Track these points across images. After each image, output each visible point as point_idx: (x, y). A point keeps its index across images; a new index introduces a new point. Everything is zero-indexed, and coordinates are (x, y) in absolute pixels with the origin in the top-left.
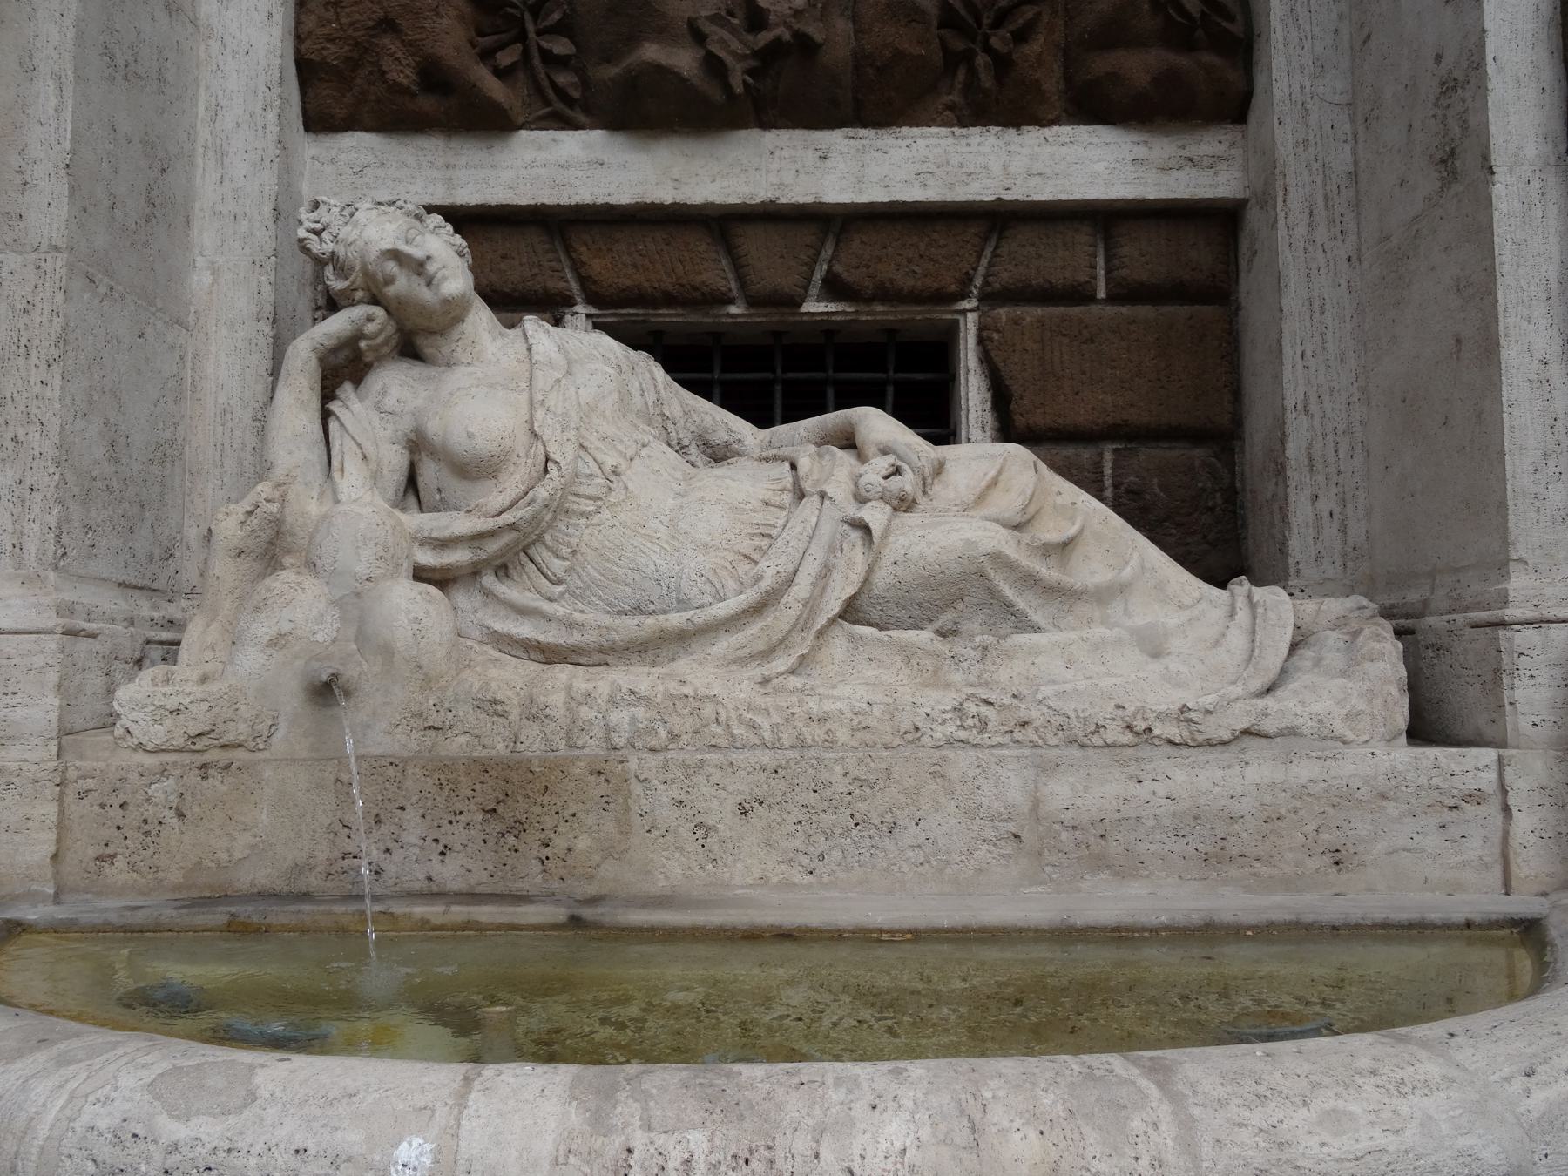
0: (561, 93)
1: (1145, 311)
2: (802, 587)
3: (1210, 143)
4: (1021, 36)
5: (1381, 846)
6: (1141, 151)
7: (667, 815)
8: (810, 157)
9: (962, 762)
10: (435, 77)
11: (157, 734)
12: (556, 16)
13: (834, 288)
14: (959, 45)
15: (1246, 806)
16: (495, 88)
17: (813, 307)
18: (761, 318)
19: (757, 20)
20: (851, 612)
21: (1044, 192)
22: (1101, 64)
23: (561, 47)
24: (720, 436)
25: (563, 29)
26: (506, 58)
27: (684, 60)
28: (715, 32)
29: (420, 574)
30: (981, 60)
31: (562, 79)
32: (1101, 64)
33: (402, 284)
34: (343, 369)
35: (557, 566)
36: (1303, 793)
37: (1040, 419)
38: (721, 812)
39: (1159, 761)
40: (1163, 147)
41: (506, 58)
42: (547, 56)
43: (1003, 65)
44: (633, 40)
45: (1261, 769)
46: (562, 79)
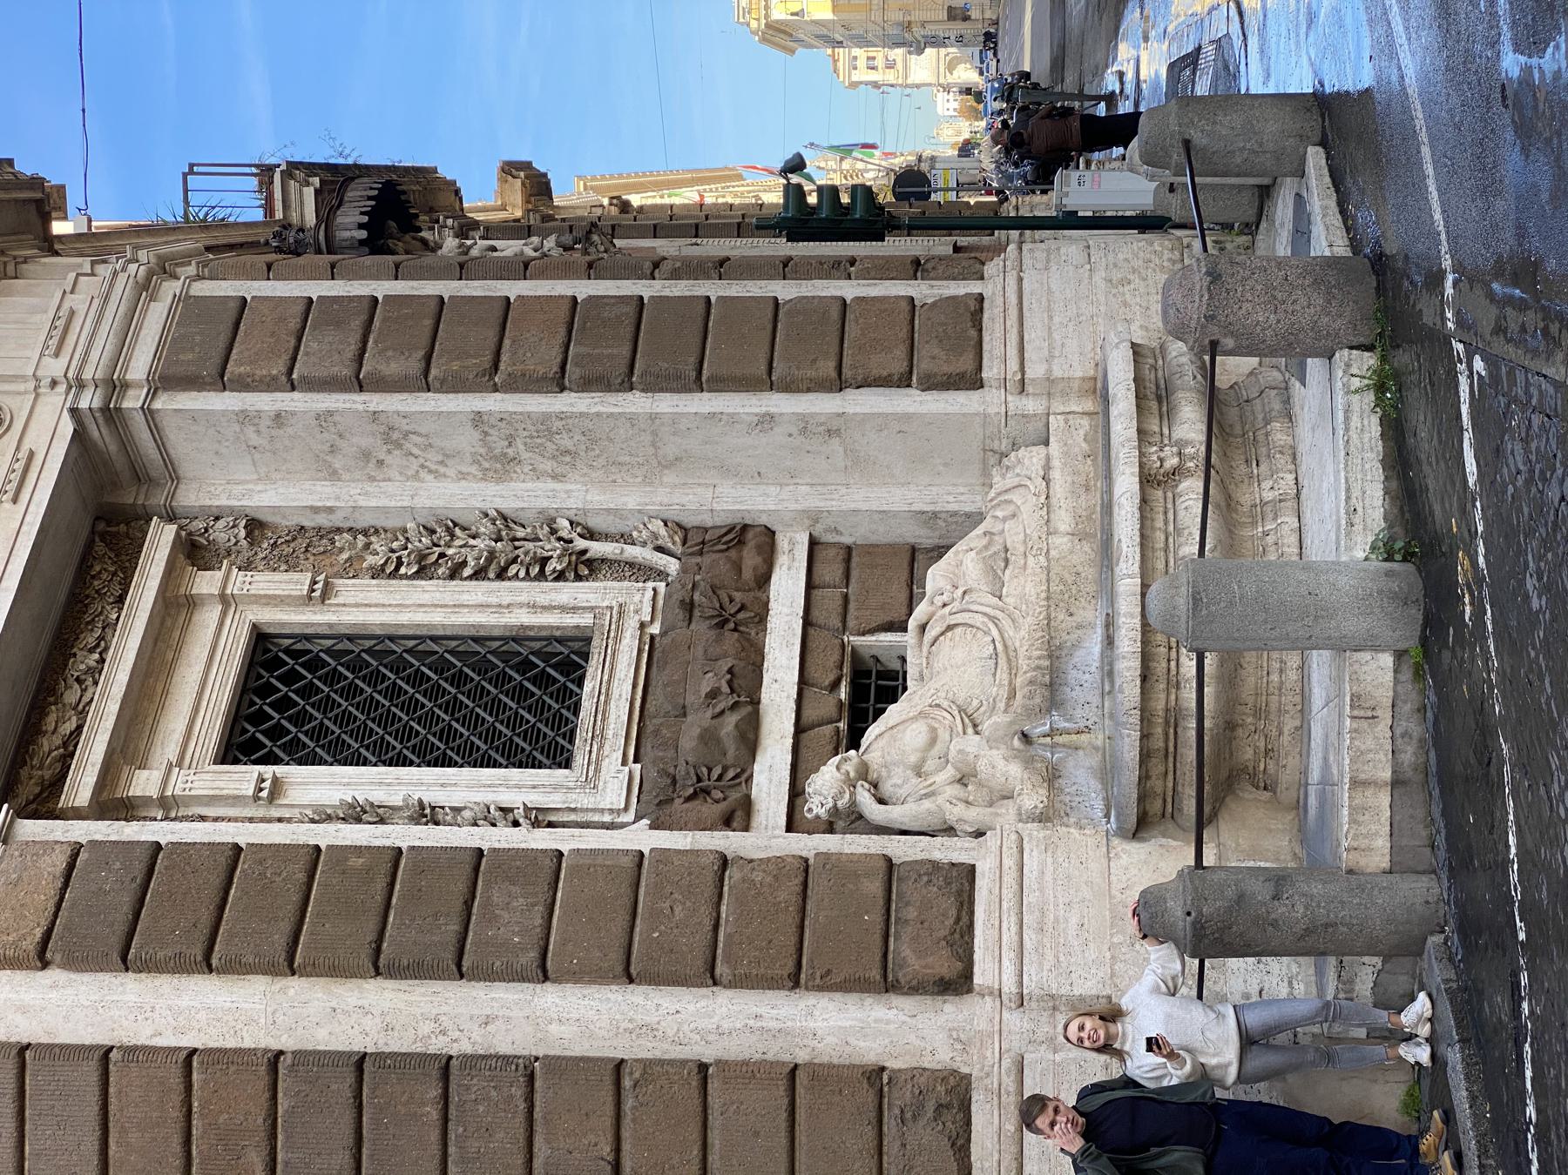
0: (737, 776)
1: (854, 574)
3: (782, 542)
5: (1084, 445)
6: (785, 568)
7: (1074, 637)
8: (776, 686)
9: (1053, 553)
11: (1043, 792)
12: (704, 770)
13: (835, 686)
14: (732, 625)
15: (1069, 479)
17: (843, 696)
18: (846, 714)
22: (747, 574)
27: (731, 720)
30: (741, 616)
31: (731, 774)
32: (747, 574)
35: (975, 703)
36: (1065, 464)
37: (904, 610)
38: (1071, 622)
39: (1054, 501)
40: (782, 560)
42: (720, 778)
44: (719, 741)
45: (1056, 475)
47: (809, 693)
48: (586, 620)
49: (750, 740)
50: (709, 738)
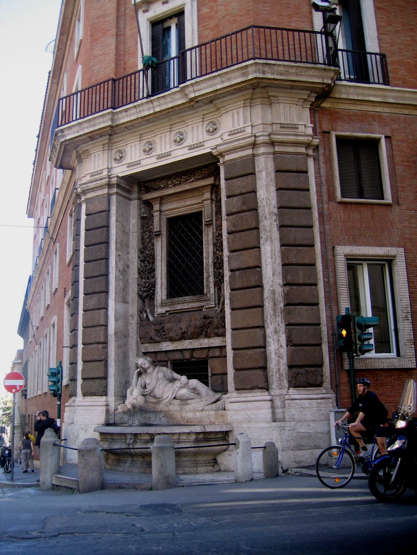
2: (170, 396)
4: (208, 328)
10: (151, 338)
16: (157, 339)
19: (181, 329)
20: (175, 398)
21: (213, 346)
23: (163, 333)
24: (176, 378)
25: (164, 331)
26: (159, 335)
27: (174, 335)
28: (178, 331)
29: (143, 395)
33: (143, 366)
34: (140, 374)
41: (159, 335)
43: (206, 332)
45: (204, 413)
46: (164, 337)
47: (190, 351)
48: (205, 292)
49: (172, 340)
50: (170, 330)
